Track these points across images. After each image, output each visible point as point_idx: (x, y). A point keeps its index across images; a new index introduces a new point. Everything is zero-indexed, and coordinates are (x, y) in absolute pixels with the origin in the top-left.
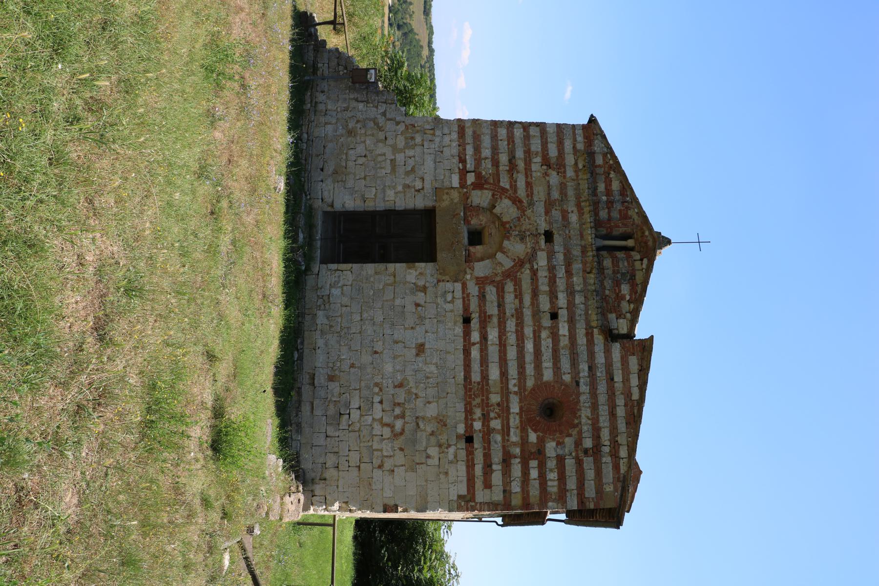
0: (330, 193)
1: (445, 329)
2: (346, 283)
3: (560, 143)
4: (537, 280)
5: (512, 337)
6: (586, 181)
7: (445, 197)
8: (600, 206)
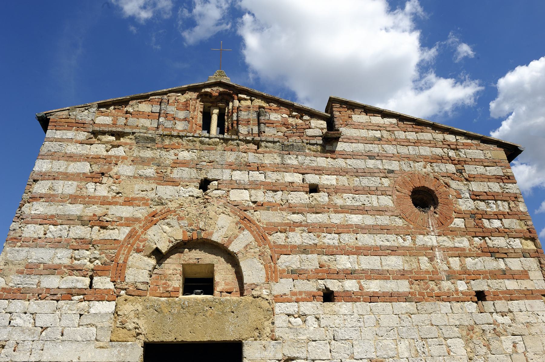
5: (347, 239)
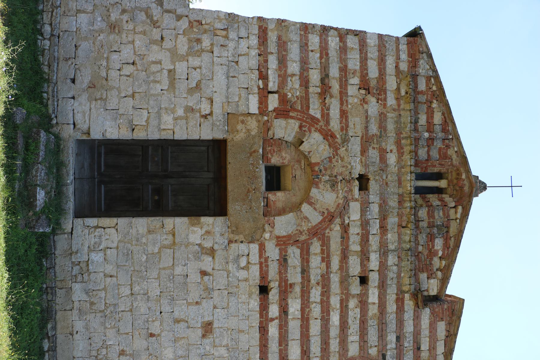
0: (84, 116)
1: (238, 303)
2: (109, 246)
4: (348, 238)
5: (316, 309)
6: (408, 113)
7: (240, 127)
8: (420, 143)
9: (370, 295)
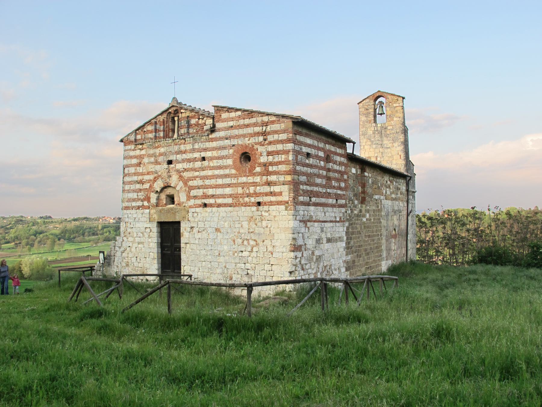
3: (131, 157)
9: (209, 155)
